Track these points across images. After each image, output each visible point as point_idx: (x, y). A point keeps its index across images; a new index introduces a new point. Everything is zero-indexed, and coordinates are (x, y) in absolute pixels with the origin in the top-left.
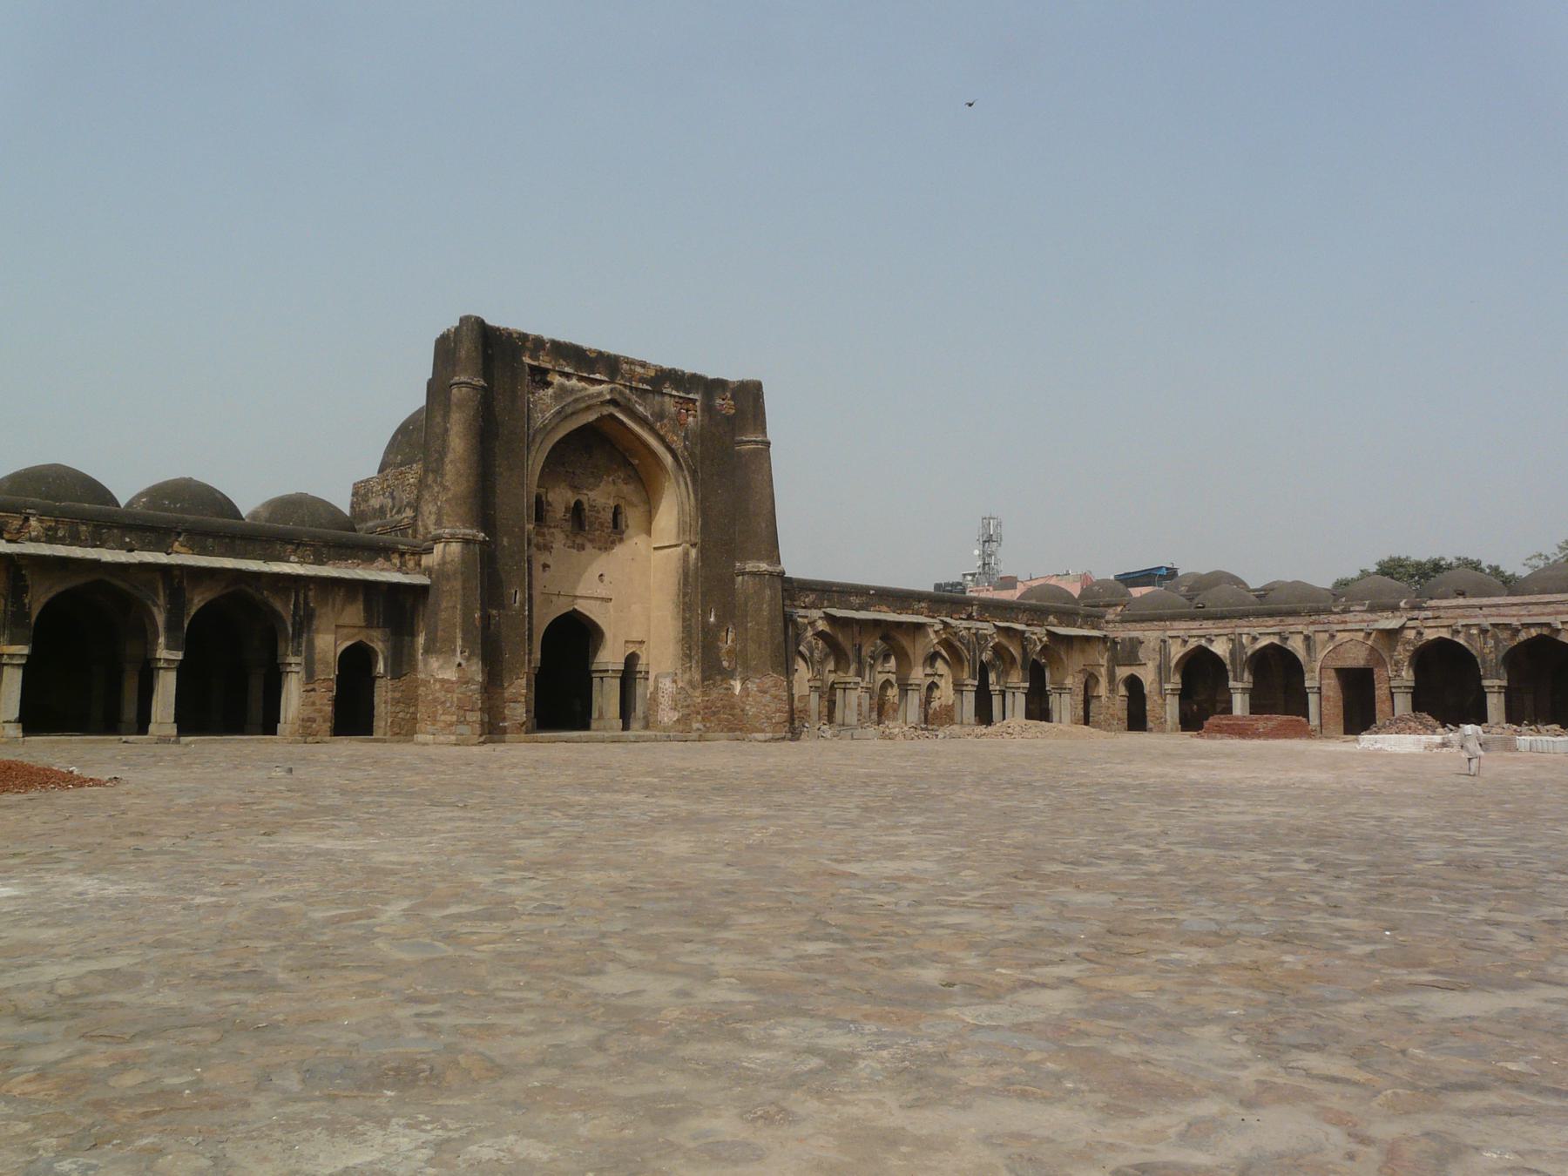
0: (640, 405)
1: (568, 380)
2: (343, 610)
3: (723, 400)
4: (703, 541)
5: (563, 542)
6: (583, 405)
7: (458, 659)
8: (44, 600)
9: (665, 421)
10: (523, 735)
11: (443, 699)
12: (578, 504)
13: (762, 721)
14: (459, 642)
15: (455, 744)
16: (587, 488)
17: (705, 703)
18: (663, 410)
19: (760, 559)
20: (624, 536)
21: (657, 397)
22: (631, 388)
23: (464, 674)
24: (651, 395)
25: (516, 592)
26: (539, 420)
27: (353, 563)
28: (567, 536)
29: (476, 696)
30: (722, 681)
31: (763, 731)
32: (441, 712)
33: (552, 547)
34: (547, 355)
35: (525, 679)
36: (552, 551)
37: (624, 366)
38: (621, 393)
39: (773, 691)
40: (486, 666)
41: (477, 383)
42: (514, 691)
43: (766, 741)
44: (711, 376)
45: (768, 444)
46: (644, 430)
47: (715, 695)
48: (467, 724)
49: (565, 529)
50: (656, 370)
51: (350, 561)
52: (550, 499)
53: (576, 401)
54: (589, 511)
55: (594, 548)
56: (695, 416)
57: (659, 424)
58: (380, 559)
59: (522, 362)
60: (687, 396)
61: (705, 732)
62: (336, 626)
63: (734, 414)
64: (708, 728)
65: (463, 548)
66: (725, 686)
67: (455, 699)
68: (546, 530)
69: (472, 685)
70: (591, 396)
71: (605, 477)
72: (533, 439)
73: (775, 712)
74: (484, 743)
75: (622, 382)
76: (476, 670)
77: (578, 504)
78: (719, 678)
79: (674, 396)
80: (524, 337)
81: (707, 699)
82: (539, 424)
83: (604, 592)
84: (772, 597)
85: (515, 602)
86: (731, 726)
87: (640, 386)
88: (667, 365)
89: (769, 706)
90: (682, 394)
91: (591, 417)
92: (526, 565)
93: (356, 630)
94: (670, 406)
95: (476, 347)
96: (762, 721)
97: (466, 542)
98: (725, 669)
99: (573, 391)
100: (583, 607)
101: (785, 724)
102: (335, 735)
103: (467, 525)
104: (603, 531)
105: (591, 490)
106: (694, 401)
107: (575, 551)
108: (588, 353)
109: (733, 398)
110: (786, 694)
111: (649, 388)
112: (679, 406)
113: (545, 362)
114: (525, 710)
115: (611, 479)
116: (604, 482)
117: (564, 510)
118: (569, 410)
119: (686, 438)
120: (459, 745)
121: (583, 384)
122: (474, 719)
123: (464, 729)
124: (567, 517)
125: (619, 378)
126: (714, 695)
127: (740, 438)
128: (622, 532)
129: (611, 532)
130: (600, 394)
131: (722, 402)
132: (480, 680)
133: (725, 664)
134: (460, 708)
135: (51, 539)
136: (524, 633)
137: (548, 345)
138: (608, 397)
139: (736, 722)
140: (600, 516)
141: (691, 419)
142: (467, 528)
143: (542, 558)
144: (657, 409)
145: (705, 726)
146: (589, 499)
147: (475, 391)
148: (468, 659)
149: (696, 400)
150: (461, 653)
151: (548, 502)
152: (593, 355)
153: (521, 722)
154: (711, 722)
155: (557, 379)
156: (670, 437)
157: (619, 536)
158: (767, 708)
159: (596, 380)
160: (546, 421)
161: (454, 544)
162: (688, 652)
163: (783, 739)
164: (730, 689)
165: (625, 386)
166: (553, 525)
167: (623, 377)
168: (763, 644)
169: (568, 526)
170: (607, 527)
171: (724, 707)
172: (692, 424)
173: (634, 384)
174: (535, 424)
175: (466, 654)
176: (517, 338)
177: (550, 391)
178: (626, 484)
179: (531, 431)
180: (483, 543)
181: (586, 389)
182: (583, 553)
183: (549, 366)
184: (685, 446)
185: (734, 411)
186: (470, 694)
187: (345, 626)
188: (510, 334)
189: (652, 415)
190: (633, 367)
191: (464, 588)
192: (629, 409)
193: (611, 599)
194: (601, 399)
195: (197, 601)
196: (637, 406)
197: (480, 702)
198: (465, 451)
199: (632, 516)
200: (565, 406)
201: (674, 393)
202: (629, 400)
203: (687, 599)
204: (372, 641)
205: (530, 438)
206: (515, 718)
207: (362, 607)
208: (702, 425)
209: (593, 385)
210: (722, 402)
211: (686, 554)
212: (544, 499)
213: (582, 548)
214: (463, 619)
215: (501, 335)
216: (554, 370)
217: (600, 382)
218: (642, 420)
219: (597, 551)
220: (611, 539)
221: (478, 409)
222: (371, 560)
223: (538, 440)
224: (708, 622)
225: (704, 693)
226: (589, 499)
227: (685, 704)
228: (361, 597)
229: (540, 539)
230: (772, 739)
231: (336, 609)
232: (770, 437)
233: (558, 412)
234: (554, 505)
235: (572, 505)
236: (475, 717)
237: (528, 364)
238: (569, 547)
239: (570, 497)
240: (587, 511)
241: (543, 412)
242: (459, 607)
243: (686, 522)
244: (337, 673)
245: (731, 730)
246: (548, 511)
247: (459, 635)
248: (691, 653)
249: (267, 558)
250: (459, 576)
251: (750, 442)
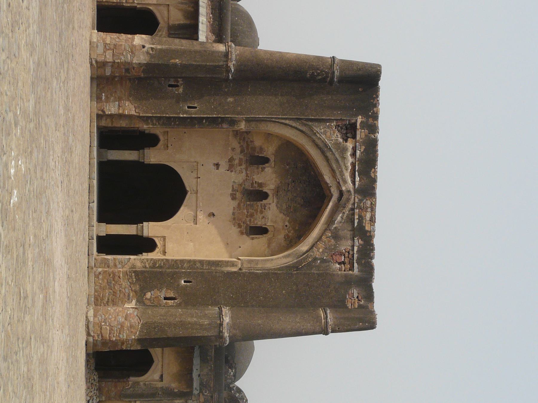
0: (342, 218)
1: (350, 155)
2: (179, 10)
3: (358, 297)
4: (244, 274)
5: (236, 181)
6: (334, 166)
7: (148, 46)
9: (332, 241)
10: (95, 111)
11: (121, 38)
12: (265, 196)
13: (103, 316)
14: (159, 47)
15: (90, 42)
16: (278, 202)
17: (117, 274)
18: (341, 240)
19: (232, 318)
20: (245, 236)
21: (349, 233)
22: (353, 209)
23: (137, 49)
24: (350, 228)
25: (196, 108)
26: (319, 129)
27: (210, 18)
28: (241, 185)
29: (123, 58)
30: (135, 292)
31: (95, 316)
32: (112, 37)
33: (232, 171)
34: (365, 135)
35: (135, 114)
36: (229, 172)
37: (369, 203)
38: (348, 200)
39: (127, 324)
40: (144, 71)
41: (335, 68)
42: (127, 105)
43: (87, 317)
44: (376, 285)
45: (326, 333)
46: (323, 224)
47: (124, 284)
48: (104, 52)
49: (246, 183)
50: (370, 232)
51: (211, 16)
52: (266, 170)
53: (337, 160)
54: (261, 204)
55: (234, 208)
56: (340, 270)
57: (330, 235)
58: (214, 37)
59: (357, 116)
60: (355, 261)
61: (95, 275)
62: (169, 5)
63: (347, 308)
64: (98, 278)
65: (222, 52)
66: (131, 295)
67: (121, 43)
68: (244, 166)
69: (131, 56)
70: (342, 174)
71: (288, 218)
72: (305, 125)
73: (110, 325)
74: (91, 64)
75: (357, 200)
76: (141, 58)
77: (265, 196)
78: (137, 287)
79: (353, 250)
80: (375, 117)
81: (121, 275)
82: (316, 129)
83: (200, 219)
84: (202, 325)
85: (189, 107)
86: (99, 300)
87: (356, 217)
88: (377, 242)
89: (115, 320)
90: (356, 256)
91: (328, 178)
92: (214, 116)
93: (166, 19)
94: (345, 246)
95: (360, 69)
96: (103, 316)
97: (226, 55)
98: (145, 295)
99: (344, 158)
101: (100, 337)
102: (97, 114)
103: (238, 57)
104: (247, 217)
105: (276, 206)
106: (352, 268)
107: (230, 191)
108: (373, 170)
109: (360, 306)
110: (125, 337)
111: (356, 225)
112: (347, 254)
113: (360, 134)
114: (113, 113)
115: (287, 223)
116: (284, 217)
117: (260, 182)
118: (329, 154)
119: (323, 261)
120: (90, 44)
121: (350, 168)
122: (108, 56)
123: (100, 50)
124: (255, 185)
125: (359, 197)
126: (125, 283)
127: (328, 311)
128: (248, 235)
129: (247, 224)
130: (345, 182)
131: (356, 295)
132: (134, 62)
133: (148, 295)
134: (115, 45)
136: (168, 114)
137: (373, 136)
138: (344, 188)
139: (102, 304)
140: (259, 214)
141: (338, 266)
142: (236, 56)
144: (341, 233)
145: (100, 273)
146: (270, 204)
147: (329, 67)
148: (148, 53)
149: (354, 271)
150: (152, 48)
151: (265, 168)
152: (372, 175)
153: (105, 110)
154: (103, 280)
155: (350, 145)
156: (321, 245)
157: (244, 231)
158: (113, 319)
159: (354, 178)
160: (318, 135)
161: (225, 48)
162: (157, 265)
163: (88, 334)
164: (129, 300)
165: (354, 204)
166: (248, 172)
167: (360, 201)
168: (165, 318)
169: (248, 186)
170: (250, 220)
171: (115, 293)
172: (334, 267)
173: (357, 211)
174: (317, 127)
175: (151, 52)
176: (374, 111)
177: (341, 140)
178: (285, 237)
179: (310, 123)
180: (228, 70)
181: (347, 170)
183: (358, 137)
184: (315, 259)
185: (350, 307)
186: (125, 54)
187: (168, 11)
188: (376, 105)
189: (335, 227)
190: (369, 210)
191: (196, 52)
192: (338, 207)
193: (196, 224)
194: (341, 183)
196: (341, 215)
197: (119, 61)
198: (288, 58)
199: (261, 241)
200: (332, 152)
201: (356, 249)
202: (344, 207)
203: (198, 265)
204: (159, 31)
205: (305, 122)
206: (108, 107)
207: (182, 22)
208: (334, 275)
209: (351, 177)
210: (356, 295)
211: (233, 264)
212: (267, 165)
213: (234, 198)
214: (175, 50)
215: (374, 99)
216: (356, 142)
217: (354, 182)
218: (331, 220)
219: (231, 211)
220: (242, 224)
221: (318, 69)
222: (213, 31)
223: (304, 128)
224: (180, 278)
225: (126, 273)
226: (270, 204)
227: (117, 263)
228: (188, 22)
229: (237, 162)
230: (89, 321)
231: (179, 5)
232: (331, 335)
233: (326, 145)
234: (263, 173)
235: (265, 190)
236: (109, 57)
237: (357, 120)
238: (233, 186)
239: (269, 188)
240: (261, 202)
241: (325, 133)
242: (182, 48)
243: (257, 264)
244: (138, 6)
245: (96, 299)
246: (258, 168)
247: (164, 47)
248: (157, 268)
250: (204, 49)
251: (326, 314)
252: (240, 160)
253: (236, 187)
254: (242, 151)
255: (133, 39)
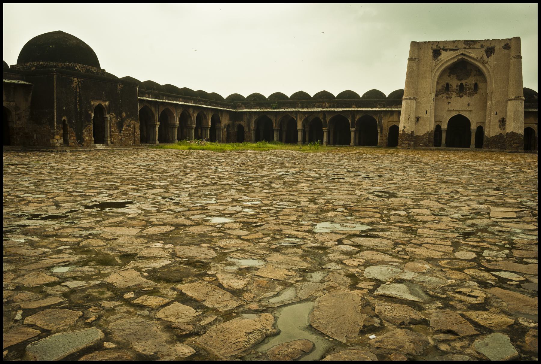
8: (329, 119)
12: (462, 84)
28: (457, 94)
68: (450, 93)
77: (462, 84)
91: (456, 60)
100: (463, 114)
107: (459, 98)
135: (330, 107)
143: (449, 100)
182: (462, 98)
195: (357, 118)
212: (449, 84)
213: (462, 96)
219: (467, 97)
229: (448, 95)
235: (459, 84)
249: (372, 107)
252: (447, 94)
253: (457, 96)
254: (443, 94)
255: (401, 134)
